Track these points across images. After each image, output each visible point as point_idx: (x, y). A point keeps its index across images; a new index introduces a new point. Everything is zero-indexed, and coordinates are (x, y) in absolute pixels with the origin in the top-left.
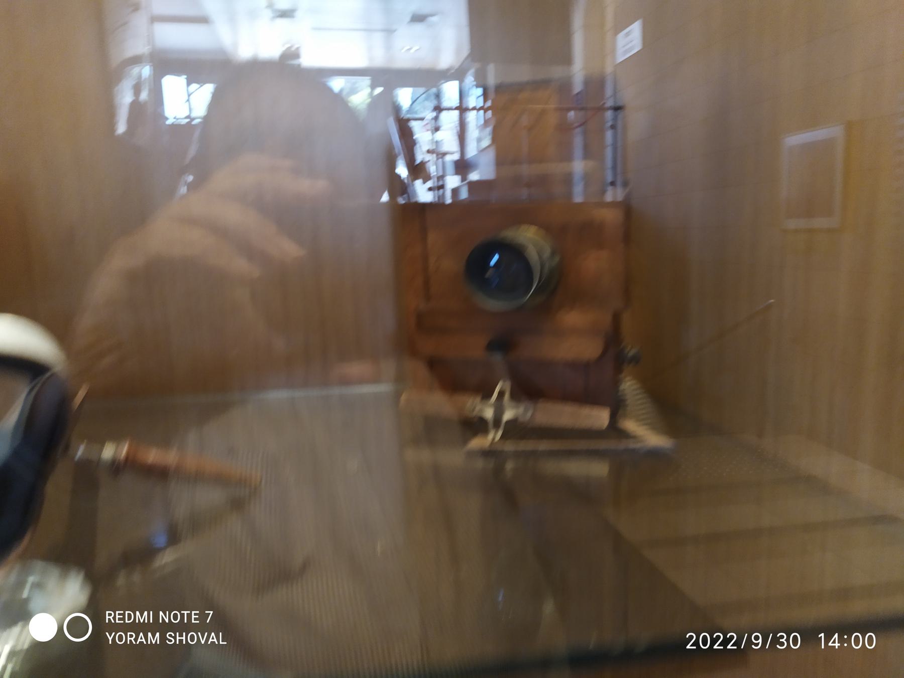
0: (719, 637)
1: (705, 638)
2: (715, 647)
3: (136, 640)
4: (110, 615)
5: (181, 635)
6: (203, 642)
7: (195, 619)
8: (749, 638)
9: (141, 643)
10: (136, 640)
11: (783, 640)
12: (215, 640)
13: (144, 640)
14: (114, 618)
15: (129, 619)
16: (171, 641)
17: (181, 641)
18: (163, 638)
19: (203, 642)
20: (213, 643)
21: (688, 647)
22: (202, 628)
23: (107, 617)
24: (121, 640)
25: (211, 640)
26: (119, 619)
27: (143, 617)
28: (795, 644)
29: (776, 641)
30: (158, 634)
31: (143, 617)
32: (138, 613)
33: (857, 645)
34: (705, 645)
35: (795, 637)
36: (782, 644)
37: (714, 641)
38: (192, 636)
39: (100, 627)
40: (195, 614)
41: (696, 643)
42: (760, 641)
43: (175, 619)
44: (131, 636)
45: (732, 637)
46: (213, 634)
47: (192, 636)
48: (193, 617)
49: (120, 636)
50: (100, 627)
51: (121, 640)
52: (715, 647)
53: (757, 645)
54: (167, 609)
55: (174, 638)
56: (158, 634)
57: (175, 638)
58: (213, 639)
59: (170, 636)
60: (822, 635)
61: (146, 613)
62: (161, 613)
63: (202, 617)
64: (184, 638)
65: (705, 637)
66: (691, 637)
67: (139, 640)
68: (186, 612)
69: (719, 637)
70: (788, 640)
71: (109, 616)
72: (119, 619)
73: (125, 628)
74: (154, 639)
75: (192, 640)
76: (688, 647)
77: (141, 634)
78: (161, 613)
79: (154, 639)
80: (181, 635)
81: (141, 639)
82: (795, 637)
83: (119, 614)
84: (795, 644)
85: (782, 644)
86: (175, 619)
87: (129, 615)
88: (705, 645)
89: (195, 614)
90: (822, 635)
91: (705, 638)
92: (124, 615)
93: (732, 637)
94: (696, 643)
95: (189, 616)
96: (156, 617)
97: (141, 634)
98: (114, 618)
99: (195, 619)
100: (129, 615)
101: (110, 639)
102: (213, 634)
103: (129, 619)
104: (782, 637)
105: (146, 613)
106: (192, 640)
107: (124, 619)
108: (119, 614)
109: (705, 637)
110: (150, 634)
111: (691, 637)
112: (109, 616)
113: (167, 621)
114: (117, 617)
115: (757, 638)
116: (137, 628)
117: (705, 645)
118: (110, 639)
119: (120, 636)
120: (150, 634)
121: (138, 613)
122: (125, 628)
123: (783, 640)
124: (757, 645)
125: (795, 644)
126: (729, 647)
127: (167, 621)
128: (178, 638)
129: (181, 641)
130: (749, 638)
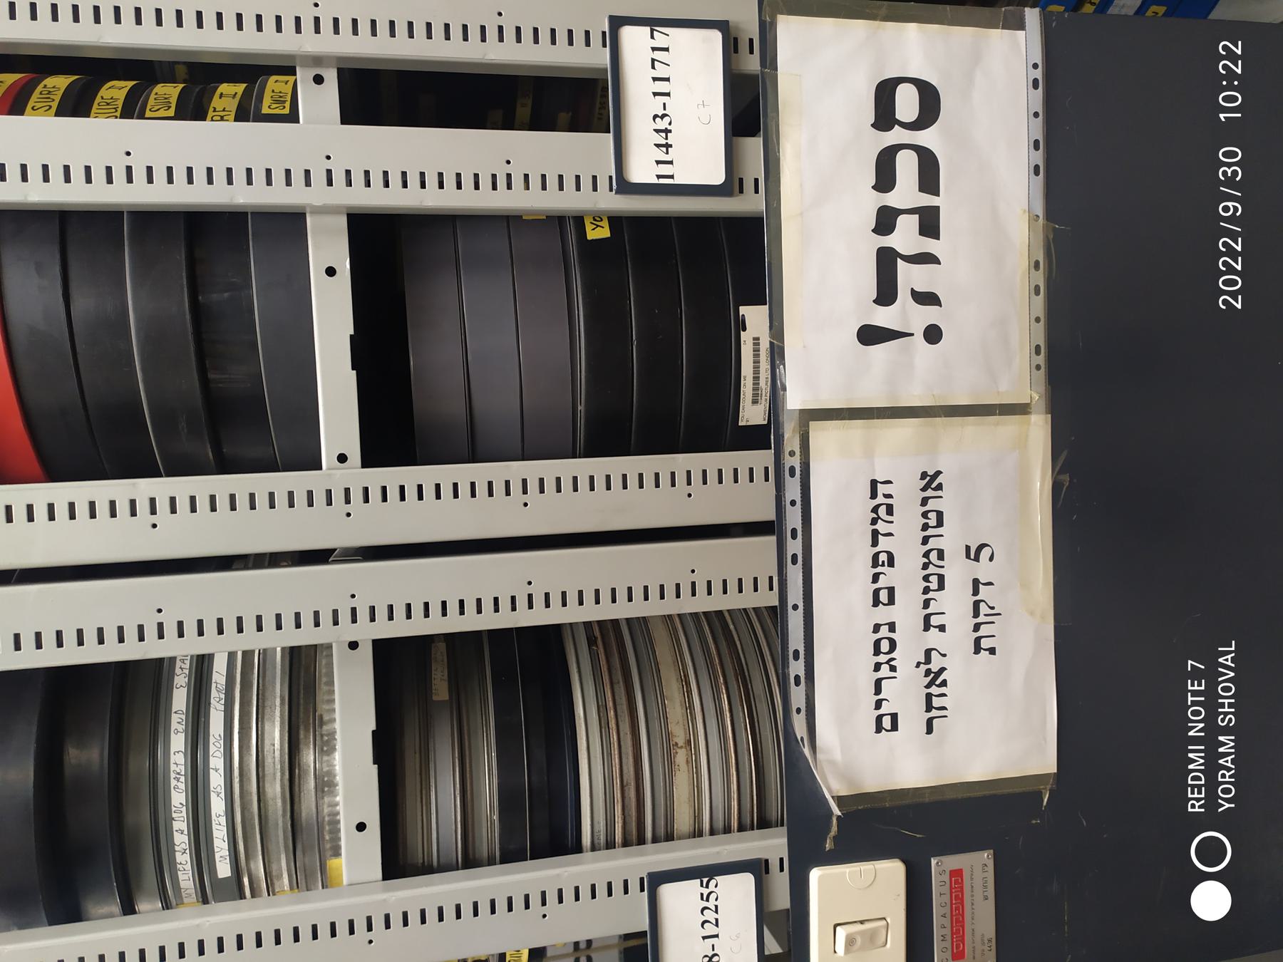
0: (1225, 263)
1: (1226, 283)
2: (1239, 268)
3: (1229, 769)
4: (1193, 806)
5: (1223, 705)
6: (1232, 674)
7: (1200, 685)
8: (1226, 220)
9: (1233, 761)
10: (1229, 769)
11: (1229, 172)
12: (1229, 657)
13: (1229, 758)
14: (1198, 800)
15: (1199, 779)
16: (1230, 720)
17: (1230, 705)
18: (1226, 731)
19: (1232, 674)
20: (1233, 660)
21: (1239, 306)
22: (1211, 675)
23: (1197, 810)
24: (1229, 791)
25: (1229, 663)
26: (1200, 793)
27: (1197, 759)
28: (1236, 155)
29: (1230, 182)
30: (1221, 738)
31: (1197, 759)
32: (1191, 767)
33: (1237, 99)
34: (1236, 283)
35: (1225, 154)
36: (1235, 173)
37: (1231, 270)
38: (1224, 689)
39: (1211, 818)
40: (1193, 685)
41: (1234, 295)
42: (1230, 204)
43: (1199, 713)
44: (1223, 776)
45: (1225, 244)
46: (1221, 660)
47: (1224, 689)
48: (1196, 688)
49: (1224, 791)
50: (1211, 818)
51: (1229, 791)
52: (1239, 268)
53: (1236, 209)
54: (1184, 725)
55: (1227, 717)
56: (1221, 738)
57: (1226, 714)
58: (1227, 660)
59: (1223, 721)
60: (1222, 116)
61: (1191, 755)
62: (1191, 733)
63: (1196, 675)
64: (1226, 701)
65: (1225, 283)
66: (1225, 302)
67: (1229, 765)
68: (1190, 699)
69: (1225, 263)
70: (1229, 165)
71: (1195, 807)
72: (1200, 793)
73: (1212, 784)
74: (1227, 743)
75: (1229, 689)
76: (1239, 306)
77: (1221, 761)
78: (1191, 733)
79: (1227, 743)
80: (1223, 705)
81: (1227, 761)
82: (1225, 154)
83: (1193, 793)
84: (1236, 155)
85: (1235, 173)
86: (1199, 713)
87: (1194, 778)
88: (1236, 283)
89: (1193, 685)
90: (1222, 116)
91: (1226, 283)
92: (1193, 787)
93: (1225, 244)
94: (1234, 295)
95: (1195, 693)
96: (1196, 741)
97: (1221, 761)
98: (1198, 800)
99: (1200, 685)
100: (1194, 778)
101: (1227, 805)
102: (1221, 660)
103: (1199, 779)
104: (1225, 173)
105: (1191, 755)
106: (1229, 689)
107: (1199, 787)
108: (1193, 793)
109: (1225, 283)
110: (1221, 750)
111: (1225, 302)
112: (1195, 807)
113: (1202, 725)
114: (1196, 796)
115: (1226, 209)
116: (1212, 767)
117: (1237, 283)
118: (1227, 805)
119: (1224, 791)
120: (1221, 750)
121: (1191, 767)
122: (1212, 784)
123: (1229, 172)
124: (1236, 209)
125: (1235, 155)
126: (1239, 249)
127: (1202, 725)
128: (1226, 710)
129: (1230, 705)
130: (1226, 220)
